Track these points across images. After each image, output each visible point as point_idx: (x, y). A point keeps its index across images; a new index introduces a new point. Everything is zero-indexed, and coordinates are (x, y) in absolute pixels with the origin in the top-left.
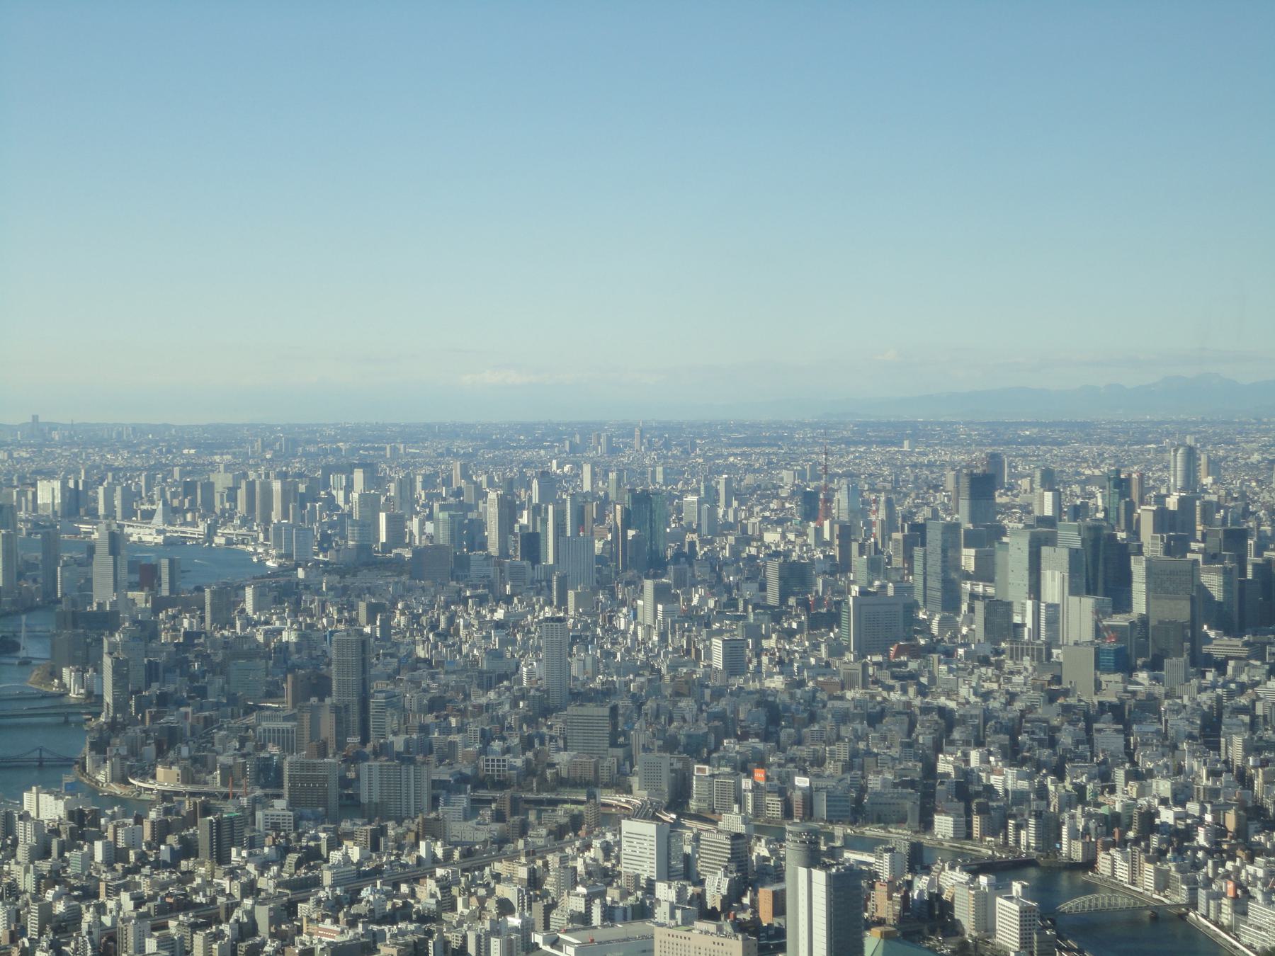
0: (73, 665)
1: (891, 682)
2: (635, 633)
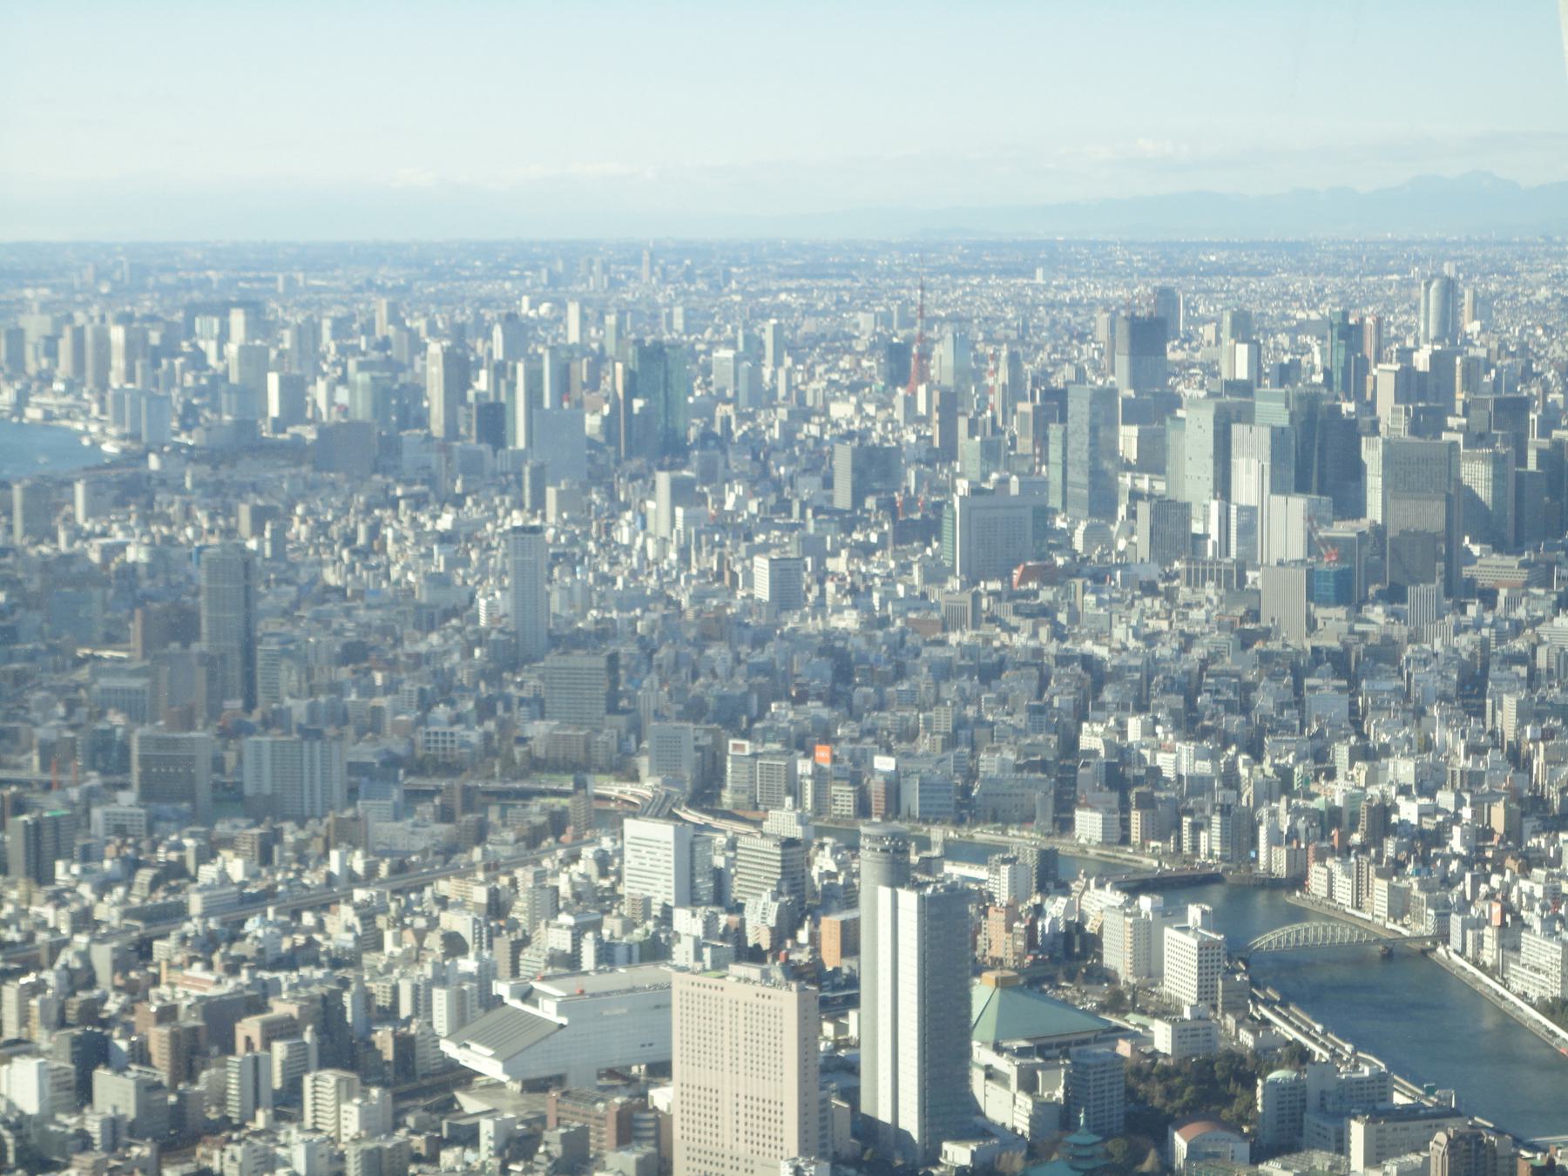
1: (1014, 621)
2: (644, 549)
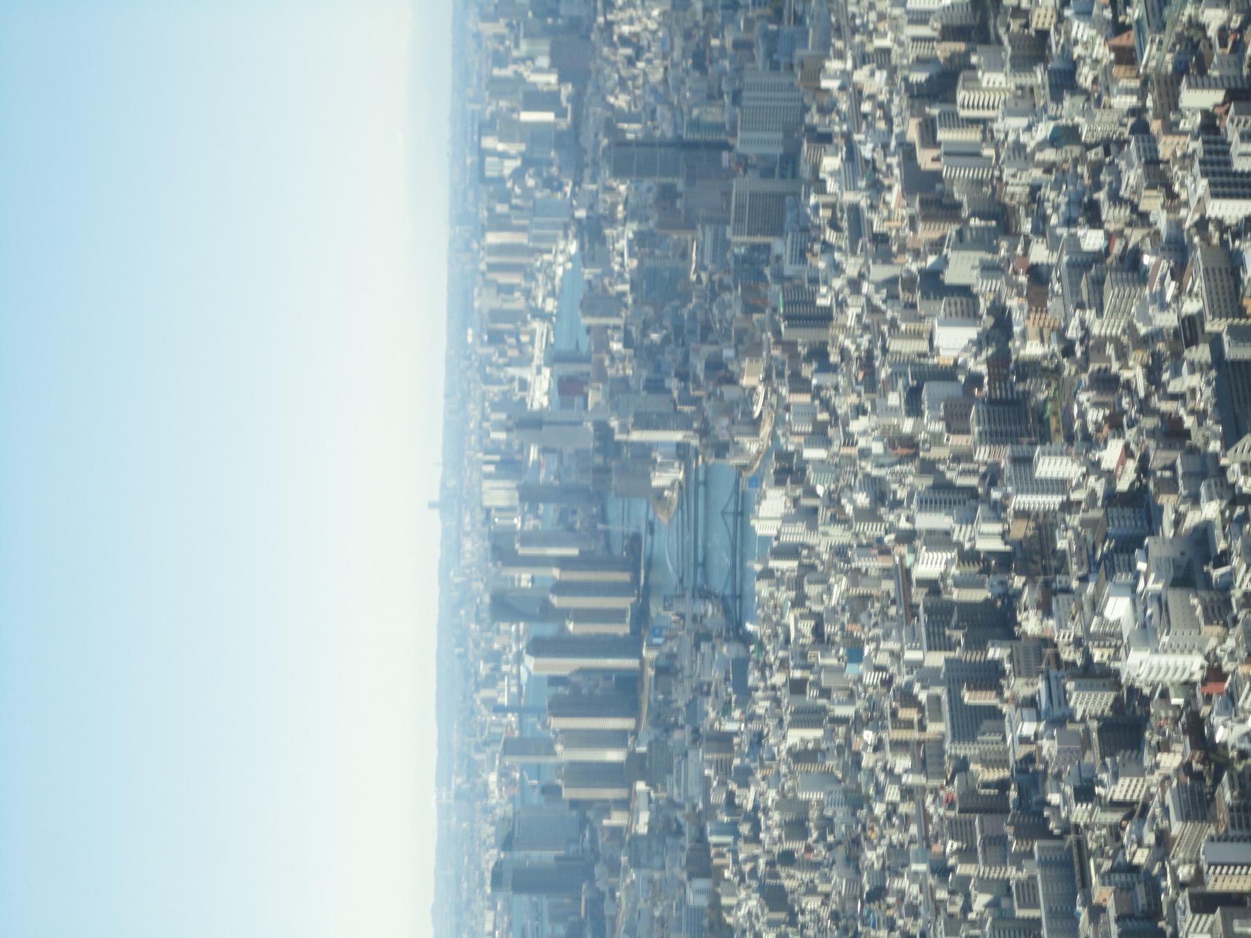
0: (649, 474)
